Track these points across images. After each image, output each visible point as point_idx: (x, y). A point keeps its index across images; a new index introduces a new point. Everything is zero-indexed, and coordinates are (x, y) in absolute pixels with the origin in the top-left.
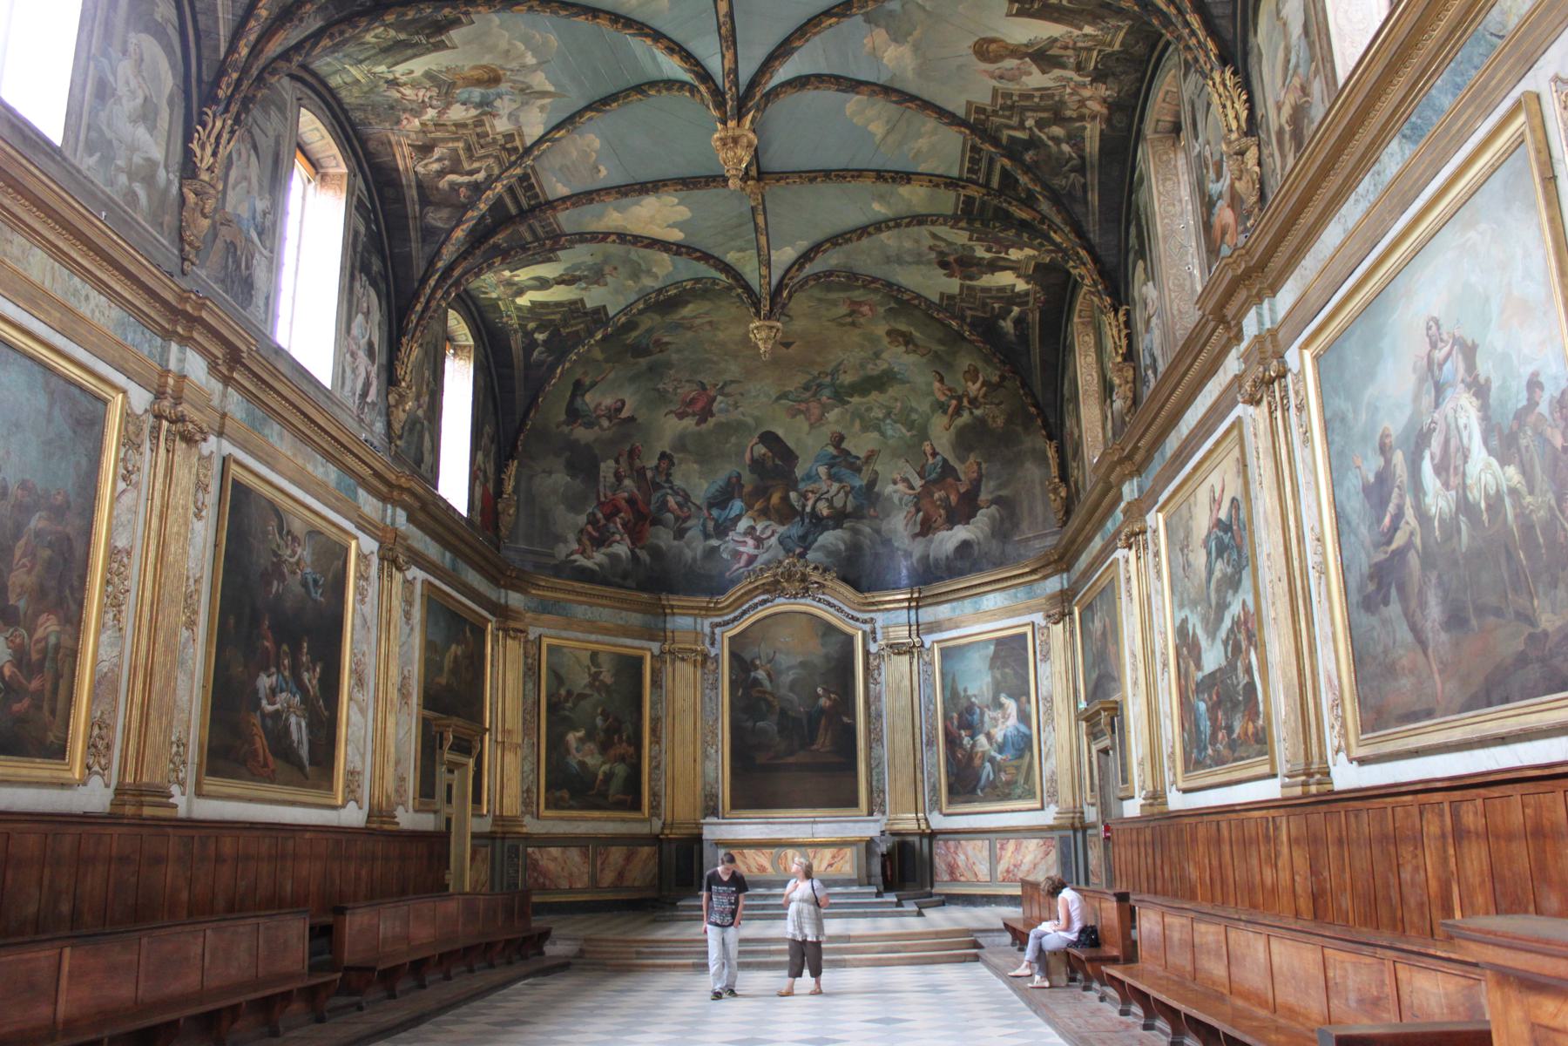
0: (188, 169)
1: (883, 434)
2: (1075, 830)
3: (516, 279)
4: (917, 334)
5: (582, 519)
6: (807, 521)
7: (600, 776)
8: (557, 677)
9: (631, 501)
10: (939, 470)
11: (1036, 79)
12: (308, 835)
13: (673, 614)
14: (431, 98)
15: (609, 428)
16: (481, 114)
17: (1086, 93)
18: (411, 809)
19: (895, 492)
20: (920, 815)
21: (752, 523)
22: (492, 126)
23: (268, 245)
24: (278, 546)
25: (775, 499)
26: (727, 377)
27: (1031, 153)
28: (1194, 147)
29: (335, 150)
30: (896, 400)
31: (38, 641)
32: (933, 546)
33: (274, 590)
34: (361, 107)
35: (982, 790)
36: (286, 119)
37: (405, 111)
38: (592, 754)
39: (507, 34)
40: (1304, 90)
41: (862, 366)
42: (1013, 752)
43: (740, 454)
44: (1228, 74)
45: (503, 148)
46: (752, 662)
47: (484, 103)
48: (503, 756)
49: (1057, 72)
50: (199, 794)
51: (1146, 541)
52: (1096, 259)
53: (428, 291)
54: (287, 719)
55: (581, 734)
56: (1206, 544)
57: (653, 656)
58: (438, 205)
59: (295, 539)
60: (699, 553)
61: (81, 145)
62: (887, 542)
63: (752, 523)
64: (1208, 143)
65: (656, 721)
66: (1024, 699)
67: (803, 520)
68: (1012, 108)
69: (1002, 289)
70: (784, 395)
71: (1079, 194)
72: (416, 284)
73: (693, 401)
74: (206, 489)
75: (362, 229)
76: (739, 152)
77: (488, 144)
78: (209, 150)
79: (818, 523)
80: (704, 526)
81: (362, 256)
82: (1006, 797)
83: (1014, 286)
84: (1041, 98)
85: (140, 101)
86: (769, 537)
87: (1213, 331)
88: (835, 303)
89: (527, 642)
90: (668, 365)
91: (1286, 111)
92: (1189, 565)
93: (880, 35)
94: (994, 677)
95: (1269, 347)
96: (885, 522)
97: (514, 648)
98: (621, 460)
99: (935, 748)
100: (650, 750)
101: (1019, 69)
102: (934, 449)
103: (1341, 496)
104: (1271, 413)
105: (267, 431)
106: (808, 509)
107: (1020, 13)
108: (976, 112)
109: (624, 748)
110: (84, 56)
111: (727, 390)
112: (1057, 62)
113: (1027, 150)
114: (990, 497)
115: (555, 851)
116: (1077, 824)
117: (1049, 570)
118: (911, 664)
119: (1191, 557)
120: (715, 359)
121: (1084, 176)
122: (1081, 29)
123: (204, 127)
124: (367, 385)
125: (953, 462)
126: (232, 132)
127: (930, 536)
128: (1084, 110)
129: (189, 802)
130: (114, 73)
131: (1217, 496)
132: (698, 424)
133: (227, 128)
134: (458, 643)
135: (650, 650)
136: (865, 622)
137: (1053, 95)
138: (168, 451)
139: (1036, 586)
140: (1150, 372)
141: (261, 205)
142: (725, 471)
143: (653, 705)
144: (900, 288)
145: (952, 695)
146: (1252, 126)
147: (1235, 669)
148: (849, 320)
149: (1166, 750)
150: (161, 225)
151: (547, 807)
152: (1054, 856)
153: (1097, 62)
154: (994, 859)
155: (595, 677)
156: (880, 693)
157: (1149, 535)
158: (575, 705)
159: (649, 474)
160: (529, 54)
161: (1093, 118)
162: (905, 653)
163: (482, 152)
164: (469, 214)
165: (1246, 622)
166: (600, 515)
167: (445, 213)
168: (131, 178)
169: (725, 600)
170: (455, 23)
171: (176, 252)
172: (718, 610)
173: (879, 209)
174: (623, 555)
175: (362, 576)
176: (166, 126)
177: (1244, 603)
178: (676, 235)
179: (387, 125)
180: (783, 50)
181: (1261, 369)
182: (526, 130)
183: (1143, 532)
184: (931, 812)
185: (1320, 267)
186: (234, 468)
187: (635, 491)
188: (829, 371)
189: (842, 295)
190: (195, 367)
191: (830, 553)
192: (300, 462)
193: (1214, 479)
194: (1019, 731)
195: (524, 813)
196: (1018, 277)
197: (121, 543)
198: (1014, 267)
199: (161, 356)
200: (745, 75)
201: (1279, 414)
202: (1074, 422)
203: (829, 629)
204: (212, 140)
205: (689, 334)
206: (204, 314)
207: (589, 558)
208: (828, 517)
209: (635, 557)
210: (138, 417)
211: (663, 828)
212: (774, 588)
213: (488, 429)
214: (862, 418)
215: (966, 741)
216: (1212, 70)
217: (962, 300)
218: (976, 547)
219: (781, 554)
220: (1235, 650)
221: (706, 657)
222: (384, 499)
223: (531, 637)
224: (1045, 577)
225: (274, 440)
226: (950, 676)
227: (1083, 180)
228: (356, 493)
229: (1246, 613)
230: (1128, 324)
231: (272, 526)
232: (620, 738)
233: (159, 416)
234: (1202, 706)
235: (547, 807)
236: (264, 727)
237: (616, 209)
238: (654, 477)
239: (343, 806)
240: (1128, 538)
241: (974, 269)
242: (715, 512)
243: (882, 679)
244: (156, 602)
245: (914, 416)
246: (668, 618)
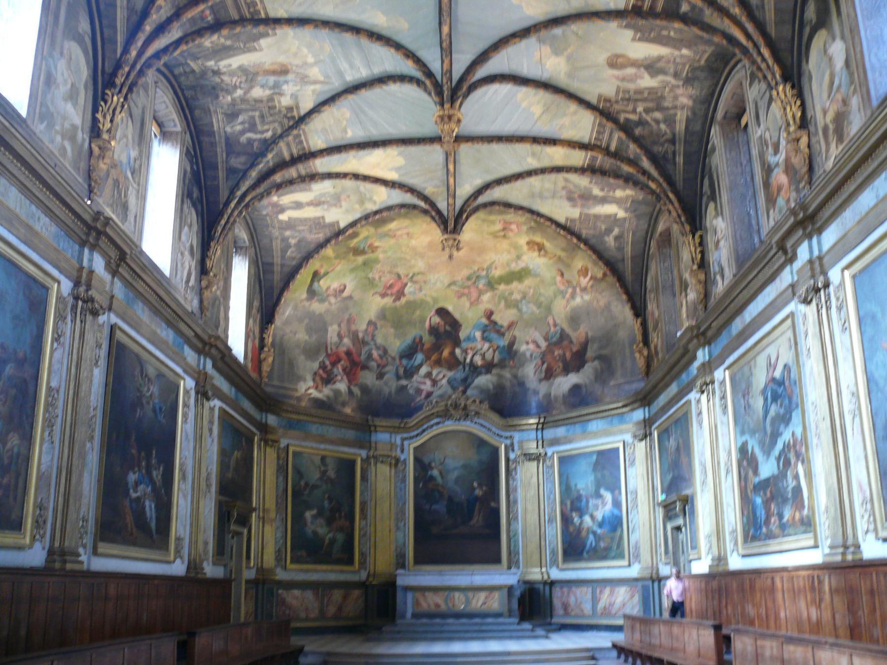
0: (95, 131)
1: (520, 310)
2: (653, 582)
3: (281, 203)
4: (547, 245)
5: (316, 365)
6: (467, 368)
7: (327, 541)
8: (298, 472)
9: (348, 353)
10: (558, 335)
11: (647, 82)
12: (156, 582)
13: (376, 431)
14: (241, 83)
15: (335, 304)
16: (273, 94)
17: (680, 91)
18: (211, 563)
19: (528, 349)
20: (544, 570)
22: (279, 102)
23: (137, 180)
24: (141, 385)
25: (446, 353)
26: (416, 270)
28: (756, 132)
29: (175, 116)
30: (530, 288)
31: (8, 451)
32: (553, 388)
33: (138, 415)
34: (193, 88)
35: (588, 552)
36: (148, 96)
37: (222, 90)
39: (297, 43)
40: (845, 102)
41: (508, 264)
43: (423, 321)
44: (788, 87)
45: (285, 116)
46: (430, 464)
47: (276, 86)
48: (263, 527)
49: (661, 78)
50: (95, 553)
51: (714, 390)
52: (680, 200)
53: (229, 211)
54: (144, 502)
55: (314, 512)
56: (764, 392)
57: (362, 460)
58: (238, 154)
59: (149, 380)
60: (393, 390)
61: (37, 116)
62: (522, 384)
63: (429, 369)
64: (768, 129)
65: (363, 504)
66: (617, 492)
68: (629, 100)
69: (608, 217)
70: (453, 283)
71: (670, 156)
72: (221, 206)
73: (391, 286)
74: (100, 347)
75: (189, 169)
76: (453, 125)
77: (275, 114)
78: (108, 118)
79: (475, 370)
81: (188, 187)
82: (604, 558)
83: (616, 215)
84: (649, 93)
85: (69, 86)
86: (441, 379)
87: (776, 254)
88: (493, 223)
89: (279, 449)
90: (376, 261)
91: (830, 115)
92: (749, 406)
93: (546, 50)
94: (596, 477)
95: (817, 265)
96: (520, 370)
97: (271, 454)
98: (342, 325)
99: (554, 524)
100: (360, 524)
101: (636, 75)
103: (872, 367)
104: (818, 311)
105: (135, 307)
106: (468, 360)
107: (640, 40)
110: (40, 57)
111: (415, 278)
112: (663, 72)
115: (296, 592)
116: (654, 576)
117: (636, 405)
118: (538, 467)
119: (751, 401)
120: (408, 258)
123: (106, 102)
124: (189, 275)
125: (568, 330)
126: (123, 106)
127: (551, 380)
129: (89, 560)
130: (56, 68)
131: (773, 362)
132: (395, 301)
133: (120, 104)
134: (238, 450)
135: (360, 455)
136: (506, 438)
138: (81, 322)
139: (626, 415)
140: (718, 278)
141: (134, 154)
143: (362, 493)
144: (539, 214)
145: (566, 488)
146: (804, 123)
147: (786, 475)
148: (502, 234)
149: (728, 529)
150: (79, 169)
151: (292, 562)
152: (637, 598)
153: (688, 73)
154: (595, 601)
155: (324, 473)
156: (516, 486)
157: (716, 385)
160: (310, 56)
161: (683, 108)
162: (534, 459)
163: (271, 119)
164: (259, 160)
165: (795, 445)
166: (327, 363)
167: (243, 159)
168: (63, 138)
169: (413, 421)
170: (266, 35)
171: (86, 187)
172: (407, 429)
173: (533, 163)
175: (186, 405)
176: (83, 103)
177: (793, 434)
178: (392, 176)
179: (209, 99)
180: (483, 57)
181: (812, 282)
182: (301, 105)
183: (713, 382)
184: (551, 567)
185: (857, 218)
186: (118, 334)
188: (485, 266)
189: (500, 217)
190: (99, 264)
191: (482, 390)
192: (153, 327)
193: (771, 351)
195: (276, 566)
196: (620, 207)
197: (54, 384)
198: (618, 202)
199: (78, 257)
200: (456, 76)
201: (824, 311)
202: (655, 305)
203: (481, 443)
204: (111, 111)
205: (392, 241)
206: (108, 230)
208: (482, 366)
209: (350, 392)
210: (64, 299)
212: (445, 415)
213: (256, 304)
214: (506, 301)
215: (576, 520)
216: (777, 84)
217: (580, 222)
218: (584, 390)
219: (450, 391)
220: (785, 463)
221: (397, 460)
222: (199, 352)
223: (282, 445)
224: (633, 410)
225: (139, 312)
226: (565, 477)
228: (183, 348)
229: (795, 441)
230: (701, 244)
231: (137, 372)
233: (76, 298)
234: (759, 500)
235: (292, 562)
236: (131, 508)
237: (354, 157)
238: (363, 337)
239: (174, 562)
240: (701, 387)
241: (591, 202)
242: (404, 362)
243: (518, 476)
244: (74, 425)
245: (542, 299)
246: (373, 434)
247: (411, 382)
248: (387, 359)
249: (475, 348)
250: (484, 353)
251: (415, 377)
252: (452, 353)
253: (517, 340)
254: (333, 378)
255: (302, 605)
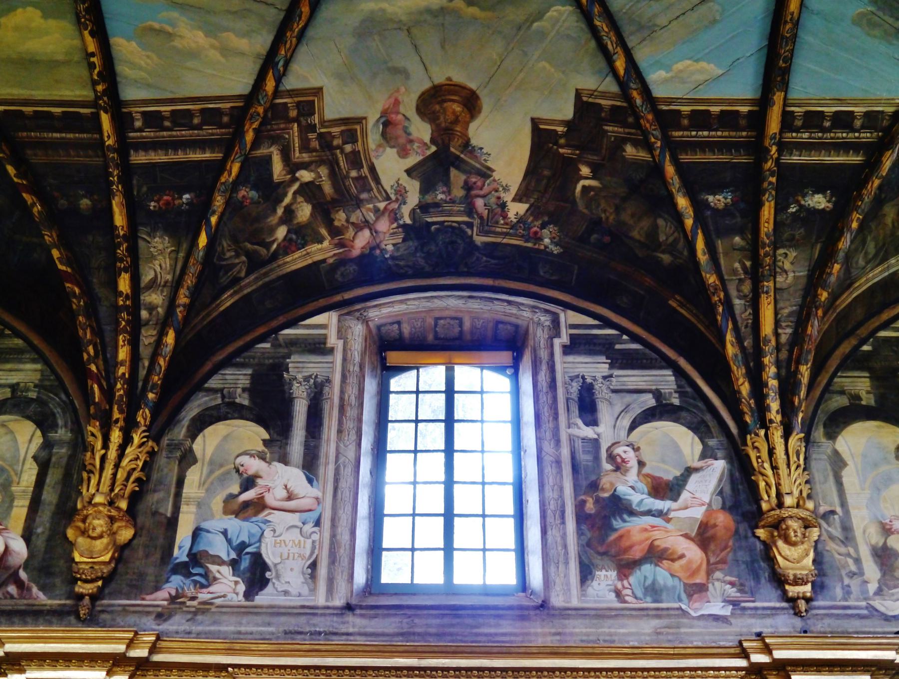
17: (383, 225)
27: (253, 194)
71: (224, 280)
84: (360, 179)
108: (298, 105)
113: (255, 187)
121: (248, 274)
122: (518, 199)
128: (351, 233)
137: (370, 190)
227: (243, 274)
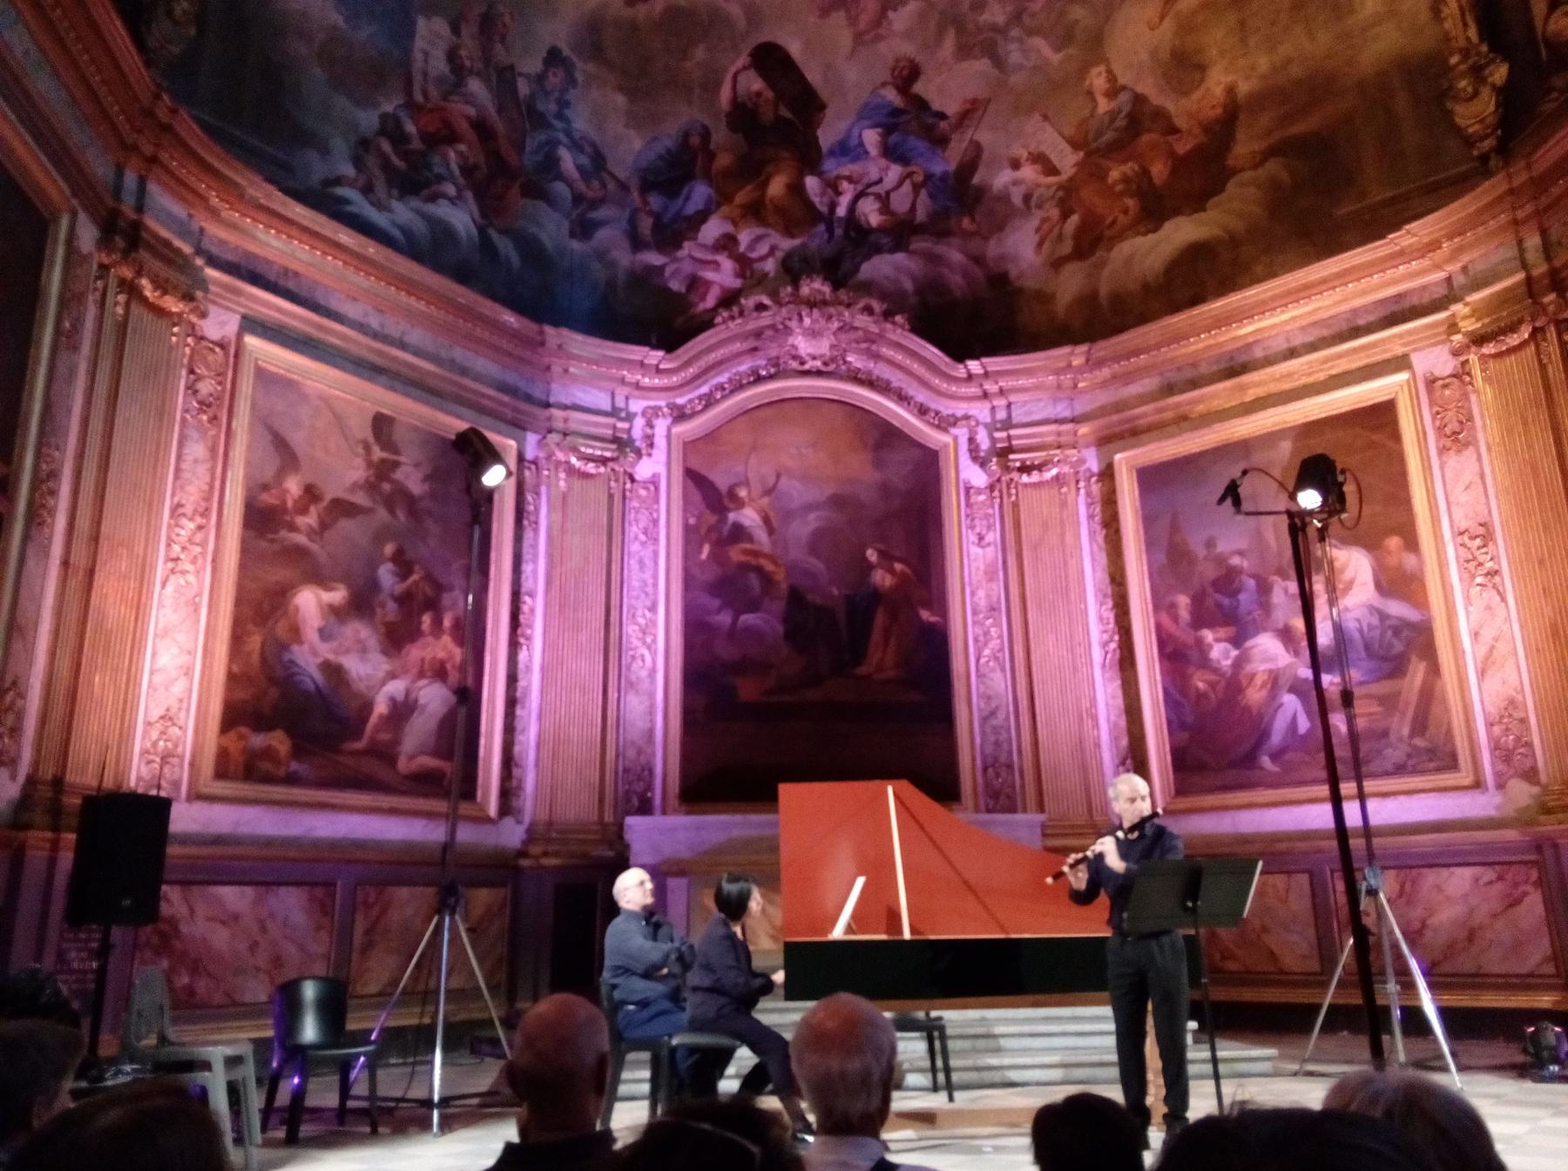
1: (998, 62)
5: (368, 120)
6: (839, 232)
7: (381, 707)
10: (1121, 122)
19: (1015, 183)
21: (730, 228)
25: (777, 187)
32: (1106, 272)
35: (1275, 757)
38: (364, 651)
42: (1367, 664)
43: (711, 86)
46: (732, 494)
62: (1000, 281)
63: (730, 228)
67: (830, 230)
80: (633, 222)
86: (763, 258)
96: (992, 243)
98: (465, 31)
102: (1112, 78)
106: (841, 211)
109: (445, 648)
114: (1258, 146)
115: (233, 896)
142: (680, 117)
155: (383, 471)
158: (324, 526)
159: (523, 88)
166: (410, 128)
174: (463, 234)
187: (492, 110)
194: (1383, 616)
203: (887, 436)
207: (380, 206)
208: (881, 229)
209: (486, 245)
211: (526, 842)
214: (961, 30)
215: (1220, 652)
232: (437, 623)
238: (532, 96)
242: (655, 201)
247: (675, 260)
248: (604, 186)
249: (862, 176)
250: (888, 193)
251: (687, 248)
252: (797, 189)
253: (985, 156)
254: (427, 184)
255: (254, 946)
